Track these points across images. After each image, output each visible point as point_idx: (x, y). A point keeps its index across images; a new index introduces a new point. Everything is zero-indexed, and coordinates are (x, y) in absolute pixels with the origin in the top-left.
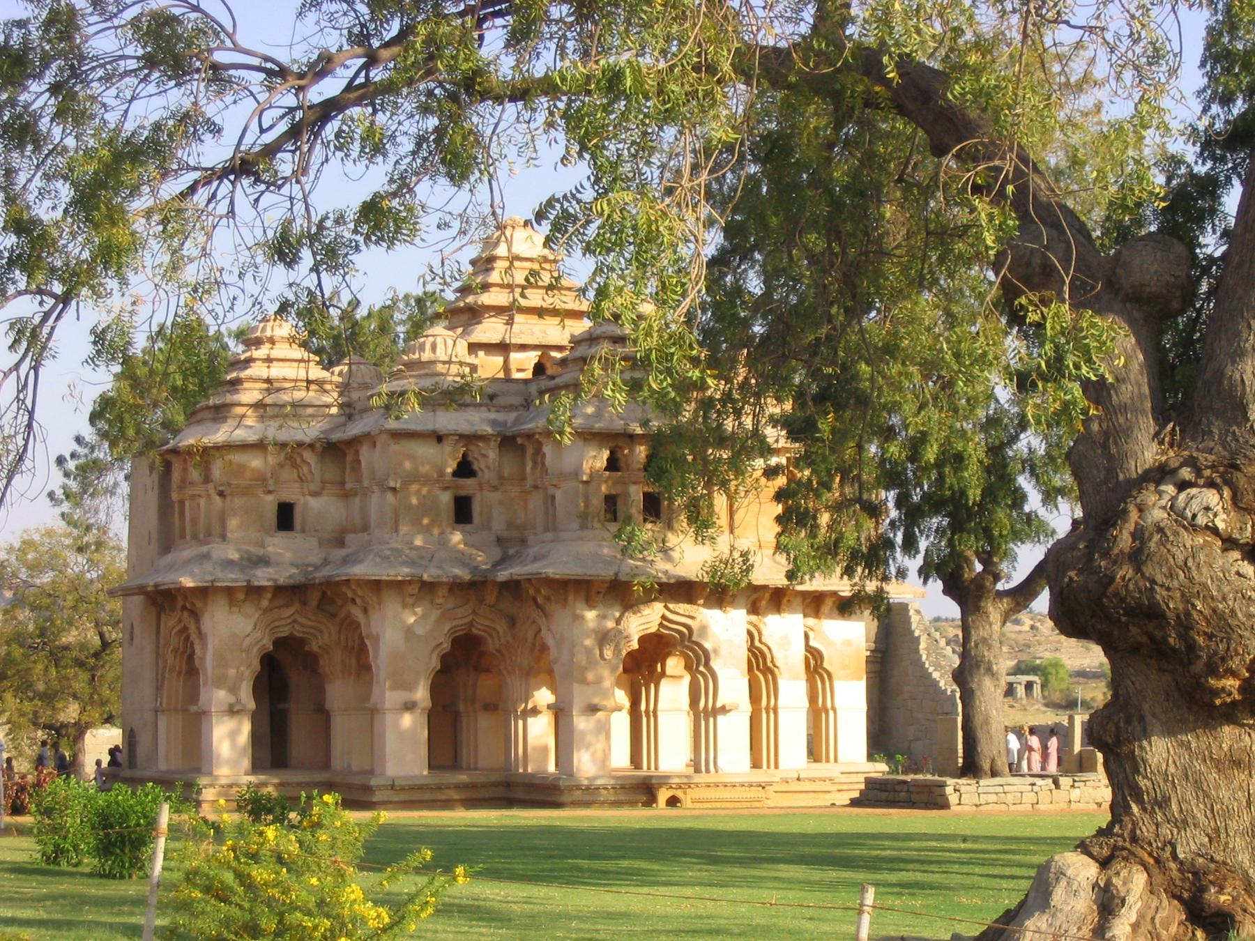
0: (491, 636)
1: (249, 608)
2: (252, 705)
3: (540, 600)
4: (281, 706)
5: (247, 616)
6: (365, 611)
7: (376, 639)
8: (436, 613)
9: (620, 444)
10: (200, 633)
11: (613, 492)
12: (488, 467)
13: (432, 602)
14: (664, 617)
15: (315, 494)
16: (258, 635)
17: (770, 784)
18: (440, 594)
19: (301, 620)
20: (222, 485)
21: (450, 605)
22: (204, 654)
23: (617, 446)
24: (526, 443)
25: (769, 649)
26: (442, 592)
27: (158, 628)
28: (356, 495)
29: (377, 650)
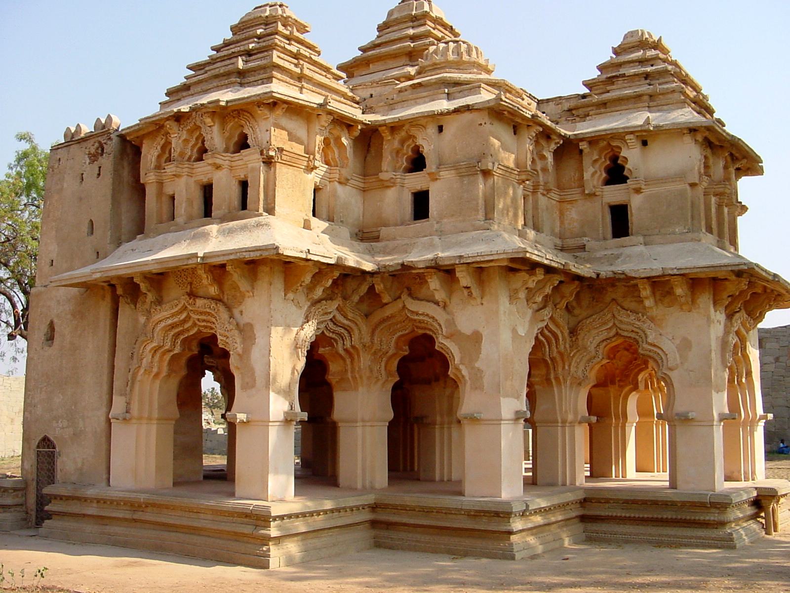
1: (302, 298)
7: (476, 338)
19: (340, 318)
22: (247, 351)
28: (388, 187)
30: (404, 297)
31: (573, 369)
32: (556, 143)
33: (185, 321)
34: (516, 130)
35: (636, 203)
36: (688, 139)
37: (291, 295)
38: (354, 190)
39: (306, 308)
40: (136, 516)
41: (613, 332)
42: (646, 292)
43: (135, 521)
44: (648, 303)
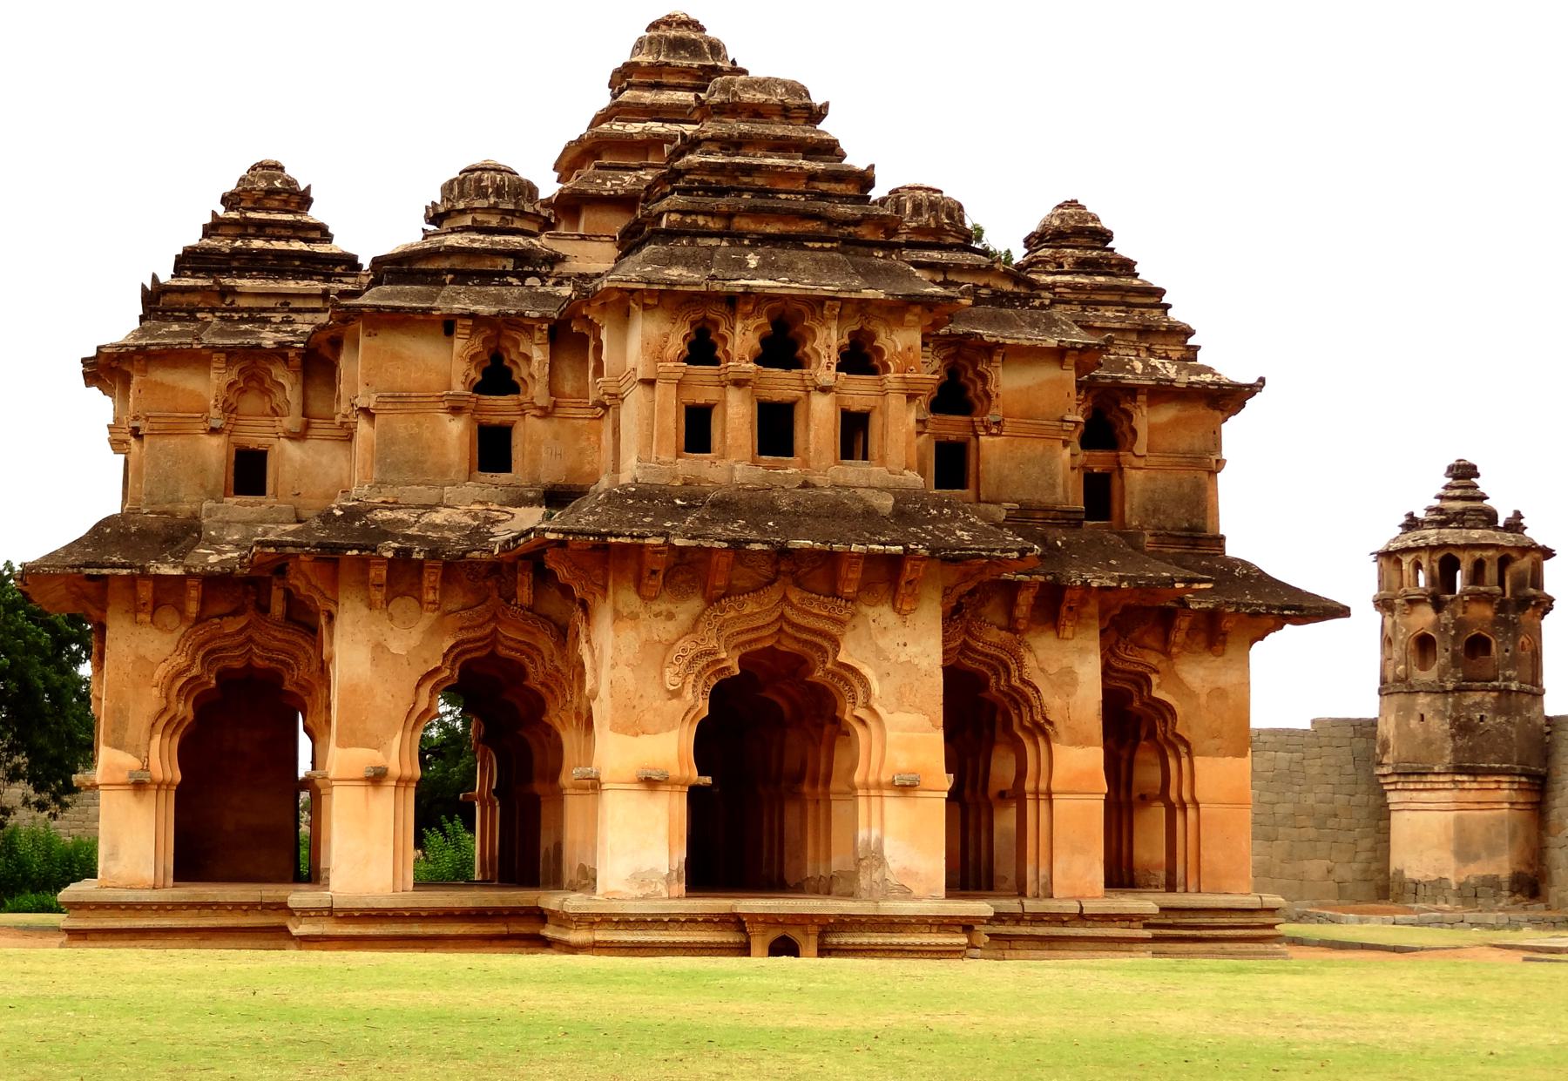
0: (533, 661)
1: (169, 617)
5: (164, 629)
8: (429, 617)
9: (711, 316)
11: (701, 401)
13: (420, 600)
15: (298, 436)
16: (182, 661)
17: (978, 920)
18: (426, 584)
19: (257, 637)
20: (136, 418)
23: (705, 317)
25: (1038, 691)
26: (431, 578)
32: (540, 330)
37: (141, 617)
38: (327, 443)
39: (184, 629)
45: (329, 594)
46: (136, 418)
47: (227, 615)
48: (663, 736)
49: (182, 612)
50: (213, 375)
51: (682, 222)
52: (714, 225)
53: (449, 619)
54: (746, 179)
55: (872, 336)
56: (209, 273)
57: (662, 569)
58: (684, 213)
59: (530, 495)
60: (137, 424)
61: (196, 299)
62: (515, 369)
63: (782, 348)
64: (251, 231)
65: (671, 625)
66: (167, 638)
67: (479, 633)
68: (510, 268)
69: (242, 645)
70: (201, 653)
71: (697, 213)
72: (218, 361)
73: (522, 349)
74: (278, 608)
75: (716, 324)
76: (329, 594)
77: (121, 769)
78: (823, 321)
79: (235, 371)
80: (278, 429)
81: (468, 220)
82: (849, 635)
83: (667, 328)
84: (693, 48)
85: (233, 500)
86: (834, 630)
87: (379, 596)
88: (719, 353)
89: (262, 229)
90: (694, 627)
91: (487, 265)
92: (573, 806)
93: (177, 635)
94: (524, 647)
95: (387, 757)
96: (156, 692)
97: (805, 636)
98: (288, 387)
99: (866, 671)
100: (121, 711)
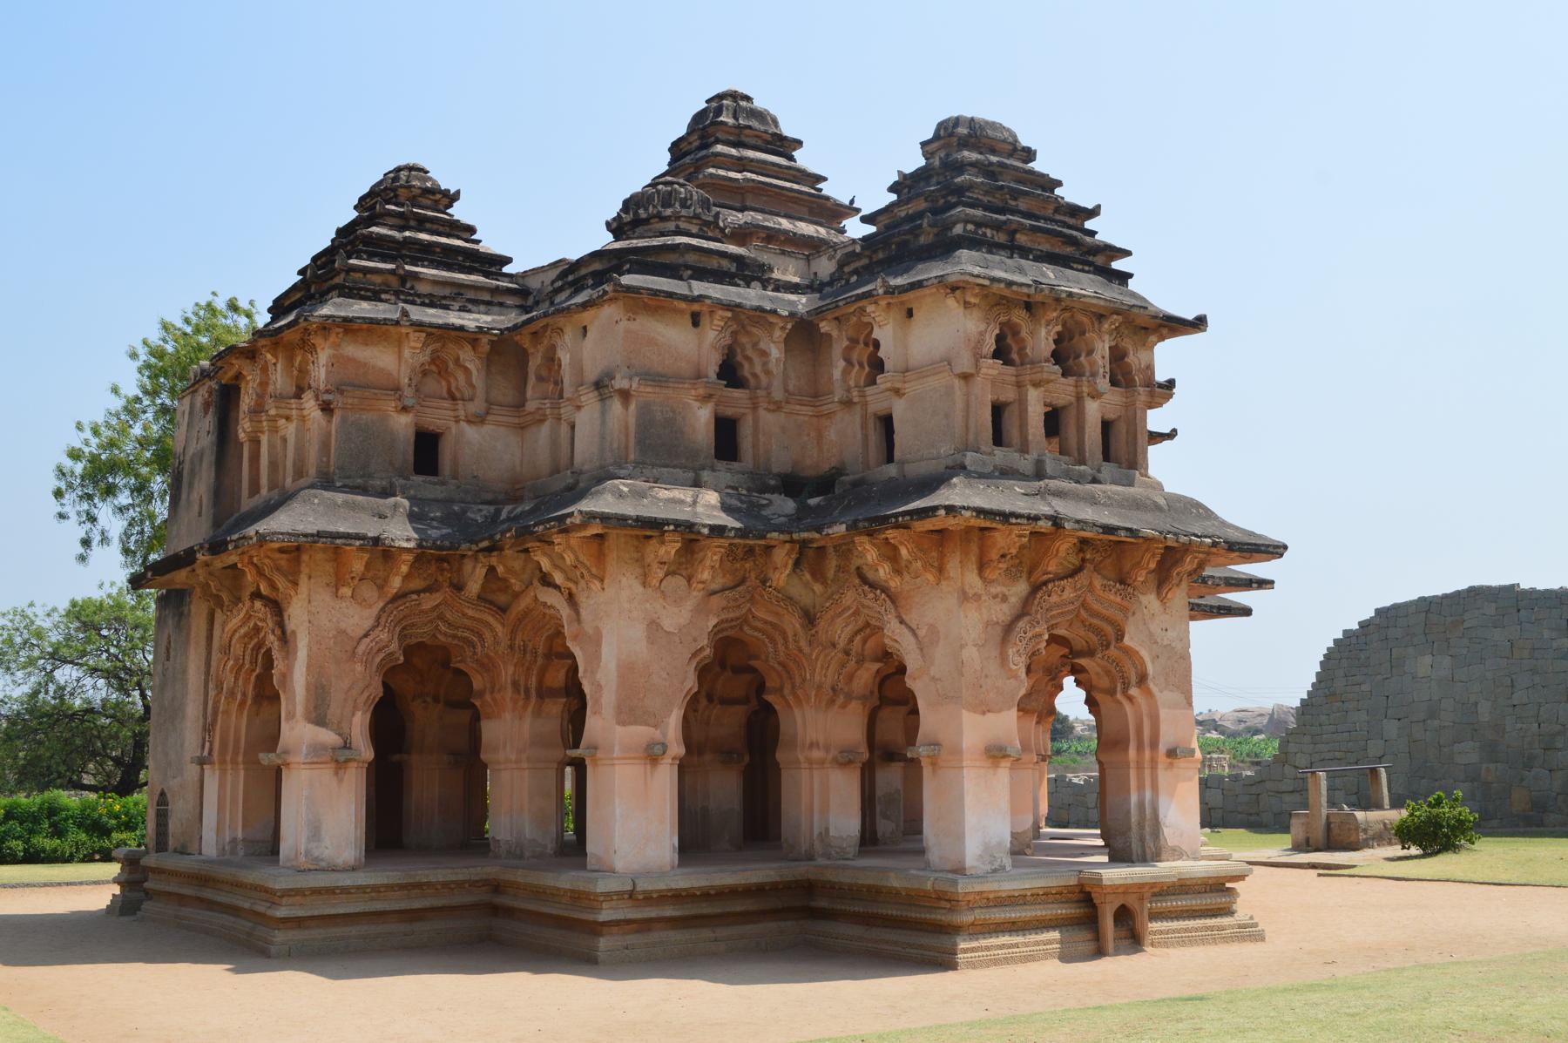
0: (773, 640)
1: (369, 591)
2: (368, 754)
3: (883, 572)
4: (396, 757)
5: (364, 603)
6: (571, 598)
7: (596, 640)
8: (697, 595)
10: (284, 632)
11: (1002, 398)
12: (768, 372)
13: (689, 579)
14: (1084, 605)
15: (478, 420)
16: (384, 636)
18: (708, 563)
19: (448, 615)
20: (327, 391)
21: (715, 586)
22: (290, 668)
24: (835, 333)
27: (210, 638)
28: (542, 421)
29: (596, 656)
30: (536, 582)
31: (817, 678)
32: (783, 328)
33: (257, 629)
34: (696, 320)
35: (899, 410)
36: (951, 302)
37: (346, 591)
38: (502, 429)
39: (381, 604)
40: (199, 894)
41: (861, 623)
42: (871, 555)
43: (201, 900)
44: (881, 572)
45: (594, 570)
46: (327, 391)
47: (424, 591)
48: (1005, 713)
49: (381, 588)
50: (407, 353)
51: (975, 232)
52: (1001, 238)
53: (715, 599)
54: (1013, 203)
55: (1124, 355)
56: (384, 258)
57: (1014, 551)
58: (978, 225)
59: (772, 482)
60: (327, 397)
61: (377, 279)
62: (746, 365)
63: (1061, 356)
64: (412, 223)
65: (1005, 607)
66: (366, 613)
67: (737, 614)
68: (733, 269)
69: (431, 621)
70: (398, 629)
71: (987, 226)
72: (416, 340)
73: (762, 345)
74: (474, 587)
75: (1015, 332)
76: (594, 570)
77: (324, 747)
78: (1100, 333)
79: (428, 350)
80: (462, 413)
81: (671, 226)
82: (1131, 619)
83: (982, 327)
84: (761, 115)
85: (419, 479)
86: (1118, 616)
87: (661, 575)
88: (1015, 356)
89: (422, 223)
90: (1023, 611)
91: (714, 263)
92: (784, 774)
93: (375, 610)
94: (769, 628)
95: (665, 735)
96: (359, 668)
97: (1095, 621)
98: (475, 373)
99: (1145, 654)
100: (323, 687)
